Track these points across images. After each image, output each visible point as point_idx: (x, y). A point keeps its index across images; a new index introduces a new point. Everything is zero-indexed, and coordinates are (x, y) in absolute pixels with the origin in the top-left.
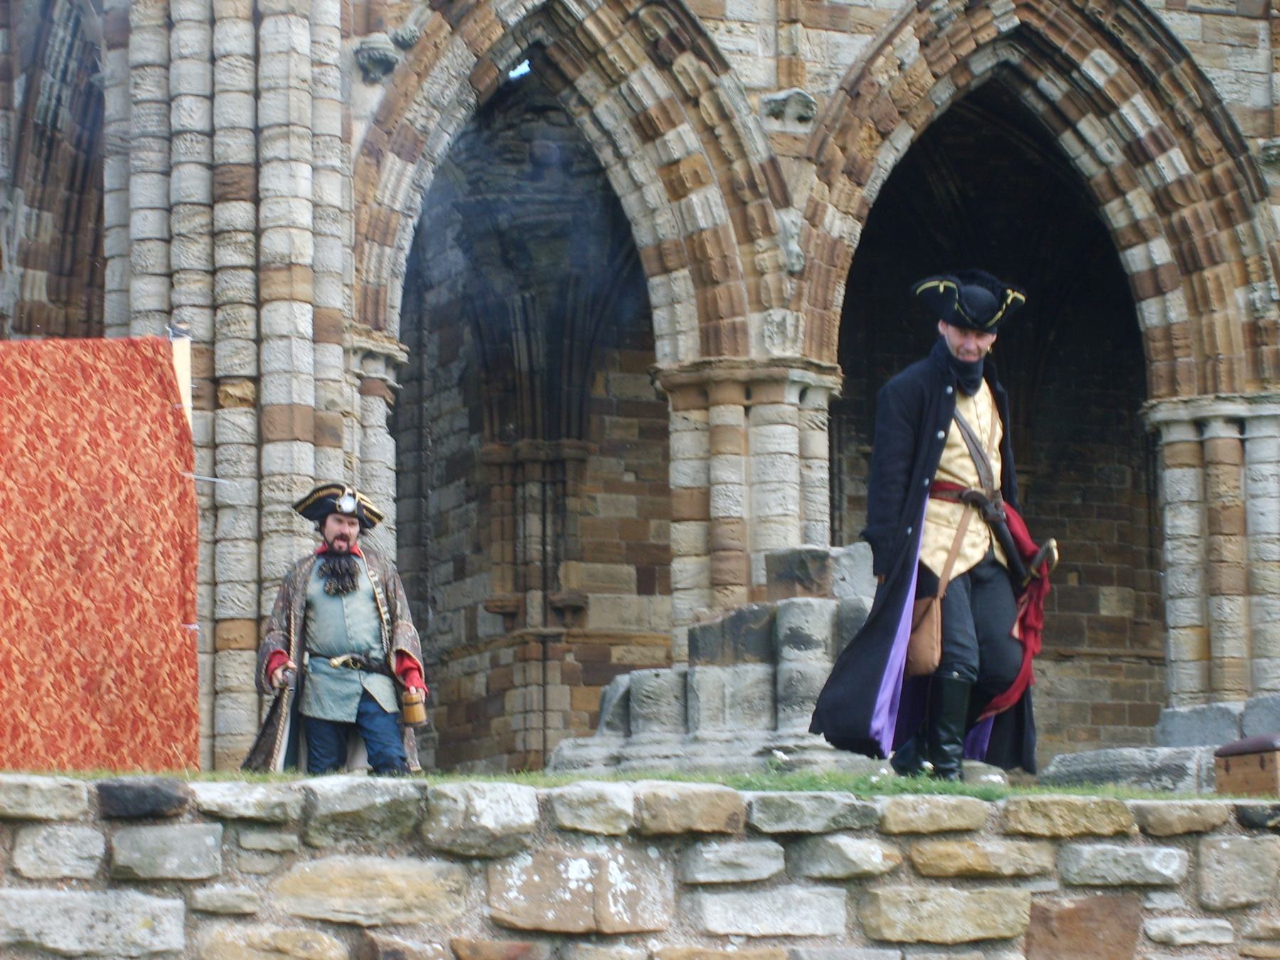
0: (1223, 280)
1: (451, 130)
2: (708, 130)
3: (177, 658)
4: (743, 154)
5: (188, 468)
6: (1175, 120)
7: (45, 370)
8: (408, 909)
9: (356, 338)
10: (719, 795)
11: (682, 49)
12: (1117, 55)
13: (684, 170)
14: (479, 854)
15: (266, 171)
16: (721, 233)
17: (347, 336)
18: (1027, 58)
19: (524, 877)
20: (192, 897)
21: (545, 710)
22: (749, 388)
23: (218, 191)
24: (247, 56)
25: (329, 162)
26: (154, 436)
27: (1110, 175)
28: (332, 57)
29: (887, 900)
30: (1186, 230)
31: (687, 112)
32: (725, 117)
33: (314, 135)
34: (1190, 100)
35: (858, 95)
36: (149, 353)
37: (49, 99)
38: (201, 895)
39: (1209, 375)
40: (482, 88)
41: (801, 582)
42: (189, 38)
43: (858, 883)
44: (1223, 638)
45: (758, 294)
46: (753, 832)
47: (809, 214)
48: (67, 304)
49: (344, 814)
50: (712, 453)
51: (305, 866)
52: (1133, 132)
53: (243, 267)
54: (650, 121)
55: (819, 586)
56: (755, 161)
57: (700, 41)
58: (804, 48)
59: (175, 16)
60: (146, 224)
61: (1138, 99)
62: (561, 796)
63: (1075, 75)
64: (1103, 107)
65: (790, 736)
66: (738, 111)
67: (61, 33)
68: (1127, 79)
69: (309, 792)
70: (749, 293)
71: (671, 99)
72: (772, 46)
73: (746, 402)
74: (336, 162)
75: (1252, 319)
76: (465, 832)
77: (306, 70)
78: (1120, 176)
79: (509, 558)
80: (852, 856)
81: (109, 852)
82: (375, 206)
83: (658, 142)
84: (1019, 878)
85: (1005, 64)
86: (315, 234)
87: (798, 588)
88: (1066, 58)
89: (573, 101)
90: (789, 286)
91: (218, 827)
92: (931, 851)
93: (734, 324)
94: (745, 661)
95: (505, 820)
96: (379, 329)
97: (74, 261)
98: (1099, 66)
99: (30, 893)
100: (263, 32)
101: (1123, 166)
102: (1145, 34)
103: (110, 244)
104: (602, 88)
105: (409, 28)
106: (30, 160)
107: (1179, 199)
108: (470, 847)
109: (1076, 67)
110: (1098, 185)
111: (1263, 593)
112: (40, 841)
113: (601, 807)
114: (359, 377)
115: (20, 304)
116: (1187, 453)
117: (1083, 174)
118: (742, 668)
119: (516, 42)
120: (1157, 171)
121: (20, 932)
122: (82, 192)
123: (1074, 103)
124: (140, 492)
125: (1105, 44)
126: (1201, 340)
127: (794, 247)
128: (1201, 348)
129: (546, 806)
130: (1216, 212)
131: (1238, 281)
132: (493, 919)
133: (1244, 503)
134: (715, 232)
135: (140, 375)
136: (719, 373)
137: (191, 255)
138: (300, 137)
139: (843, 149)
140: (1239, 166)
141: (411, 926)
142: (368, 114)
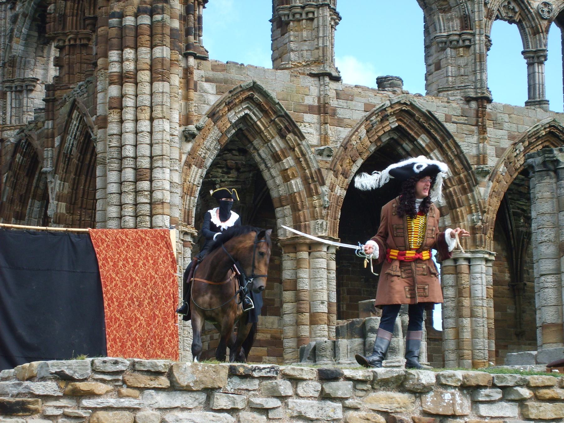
1: (212, 158)
2: (297, 160)
3: (172, 335)
4: (309, 167)
5: (175, 272)
7: (129, 239)
8: (401, 408)
10: (485, 375)
11: (289, 132)
13: (289, 172)
14: (419, 392)
15: (155, 171)
18: (399, 137)
20: (344, 403)
23: (138, 177)
24: (148, 132)
26: (164, 262)
28: (176, 133)
29: (531, 406)
30: (451, 195)
31: (291, 153)
32: (303, 155)
36: (163, 234)
37: (69, 144)
38: (347, 402)
42: (129, 126)
43: (521, 402)
44: (464, 332)
45: (314, 214)
46: (494, 386)
48: (73, 214)
49: (384, 379)
51: (373, 395)
53: (147, 203)
54: (278, 155)
58: (329, 132)
59: (123, 118)
60: (113, 188)
61: (436, 151)
63: (415, 143)
67: (75, 123)
68: (432, 145)
69: (374, 372)
76: (417, 385)
77: (168, 137)
80: (521, 393)
81: (322, 388)
85: (392, 139)
86: (171, 192)
87: (371, 314)
88: (413, 137)
89: (252, 149)
90: (324, 212)
91: (351, 382)
92: (543, 392)
94: (355, 338)
95: (428, 381)
96: (189, 225)
97: (75, 200)
99: (302, 401)
100: (154, 124)
102: (438, 130)
103: (98, 195)
105: (201, 123)
106: (61, 165)
108: (418, 389)
109: (416, 140)
111: (477, 317)
112: (304, 386)
113: (454, 378)
114: (183, 240)
115: (56, 214)
118: (354, 340)
119: (234, 128)
121: (300, 412)
122: (79, 175)
124: (159, 281)
127: (326, 198)
129: (438, 377)
132: (424, 411)
134: (299, 193)
135: (159, 241)
137: (129, 199)
138: (167, 159)
139: (341, 166)
141: (401, 412)
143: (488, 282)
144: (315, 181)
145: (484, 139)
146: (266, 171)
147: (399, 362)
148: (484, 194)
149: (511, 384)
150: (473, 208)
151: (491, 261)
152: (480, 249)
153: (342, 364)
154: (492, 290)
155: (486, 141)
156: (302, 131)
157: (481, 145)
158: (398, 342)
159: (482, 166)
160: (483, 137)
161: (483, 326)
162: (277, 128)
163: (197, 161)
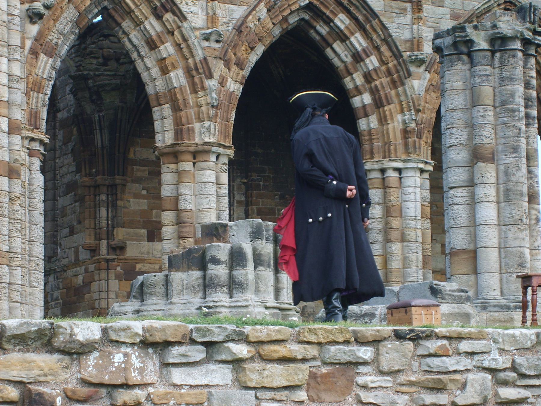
0: (392, 111)
1: (68, 44)
2: (178, 46)
4: (193, 56)
6: (373, 44)
8: (45, 375)
9: (27, 132)
10: (178, 326)
11: (167, 11)
12: (349, 17)
13: (167, 62)
14: (76, 352)
16: (183, 89)
17: (23, 131)
18: (312, 17)
19: (95, 361)
21: (108, 291)
22: (195, 154)
25: (15, 57)
27: (346, 66)
28: (16, 12)
29: (249, 370)
30: (378, 91)
31: (169, 38)
32: (185, 40)
33: (9, 45)
34: (379, 36)
35: (241, 31)
39: (387, 151)
40: (81, 26)
41: (216, 237)
43: (237, 363)
44: (392, 260)
45: (199, 115)
46: (193, 342)
47: (220, 82)
49: (18, 335)
50: (179, 182)
52: (356, 49)
54: (153, 41)
55: (224, 238)
56: (198, 59)
57: (174, 8)
58: (219, 11)
61: (358, 35)
62: (111, 326)
63: (332, 24)
64: (343, 38)
65: (211, 302)
66: (191, 38)
68: (353, 27)
70: (195, 114)
71: (162, 32)
72: (205, 10)
73: (194, 161)
74: (18, 57)
75: (404, 127)
78: (350, 67)
79: (93, 226)
80: (234, 351)
82: (35, 76)
83: (156, 50)
84: (304, 360)
85: (303, 19)
86: (9, 88)
87: (215, 239)
88: (328, 17)
89: (120, 33)
90: (212, 112)
92: (268, 349)
93: (188, 127)
94: (192, 270)
95: (88, 337)
96: (37, 129)
98: (342, 21)
101: (351, 63)
102: (360, 8)
104: (133, 27)
107: (375, 77)
108: (73, 349)
109: (332, 21)
110: (341, 70)
113: (129, 331)
114: (28, 149)
116: (377, 183)
117: (335, 66)
118: (191, 273)
119: (96, 7)
120: (365, 65)
123: (332, 37)
125: (345, 12)
126: (383, 136)
127: (214, 95)
128: (384, 139)
129: (105, 331)
130: (389, 82)
131: (399, 112)
132: (81, 379)
133: (401, 203)
134: (181, 89)
136: (182, 148)
139: (235, 54)
140: (399, 64)
141: (46, 382)
142: (32, 37)
143: (423, 198)
144: (200, 74)
145: (420, 19)
146: (140, 61)
147: (247, 300)
148: (419, 88)
149: (218, 339)
150: (404, 106)
151: (427, 171)
152: (413, 157)
153: (175, 304)
154: (429, 209)
155: (422, 22)
156: (183, 9)
157: (415, 27)
158: (246, 275)
159: (416, 53)
160: (418, 17)
161: (417, 252)
162: (151, 7)
163: (46, 48)
